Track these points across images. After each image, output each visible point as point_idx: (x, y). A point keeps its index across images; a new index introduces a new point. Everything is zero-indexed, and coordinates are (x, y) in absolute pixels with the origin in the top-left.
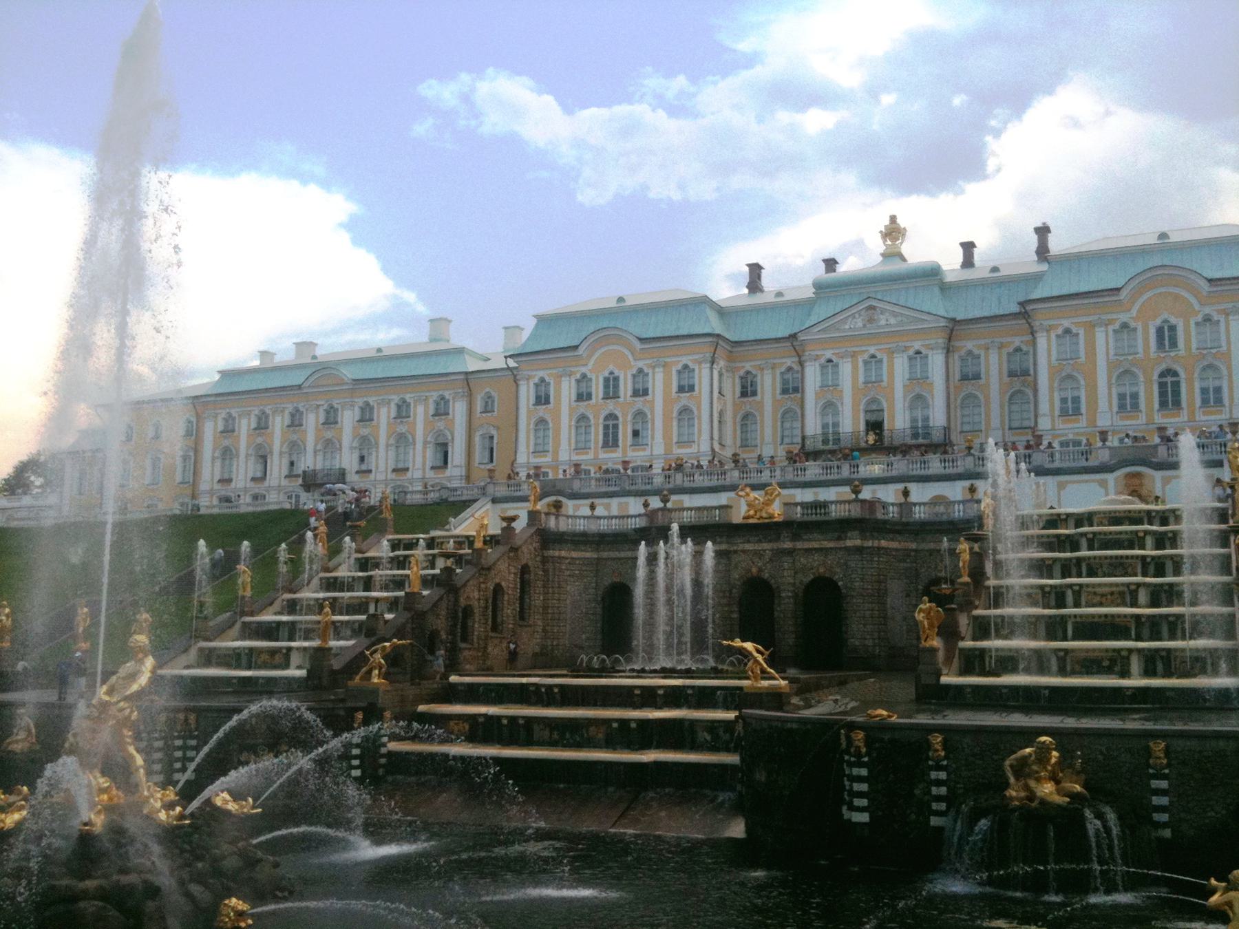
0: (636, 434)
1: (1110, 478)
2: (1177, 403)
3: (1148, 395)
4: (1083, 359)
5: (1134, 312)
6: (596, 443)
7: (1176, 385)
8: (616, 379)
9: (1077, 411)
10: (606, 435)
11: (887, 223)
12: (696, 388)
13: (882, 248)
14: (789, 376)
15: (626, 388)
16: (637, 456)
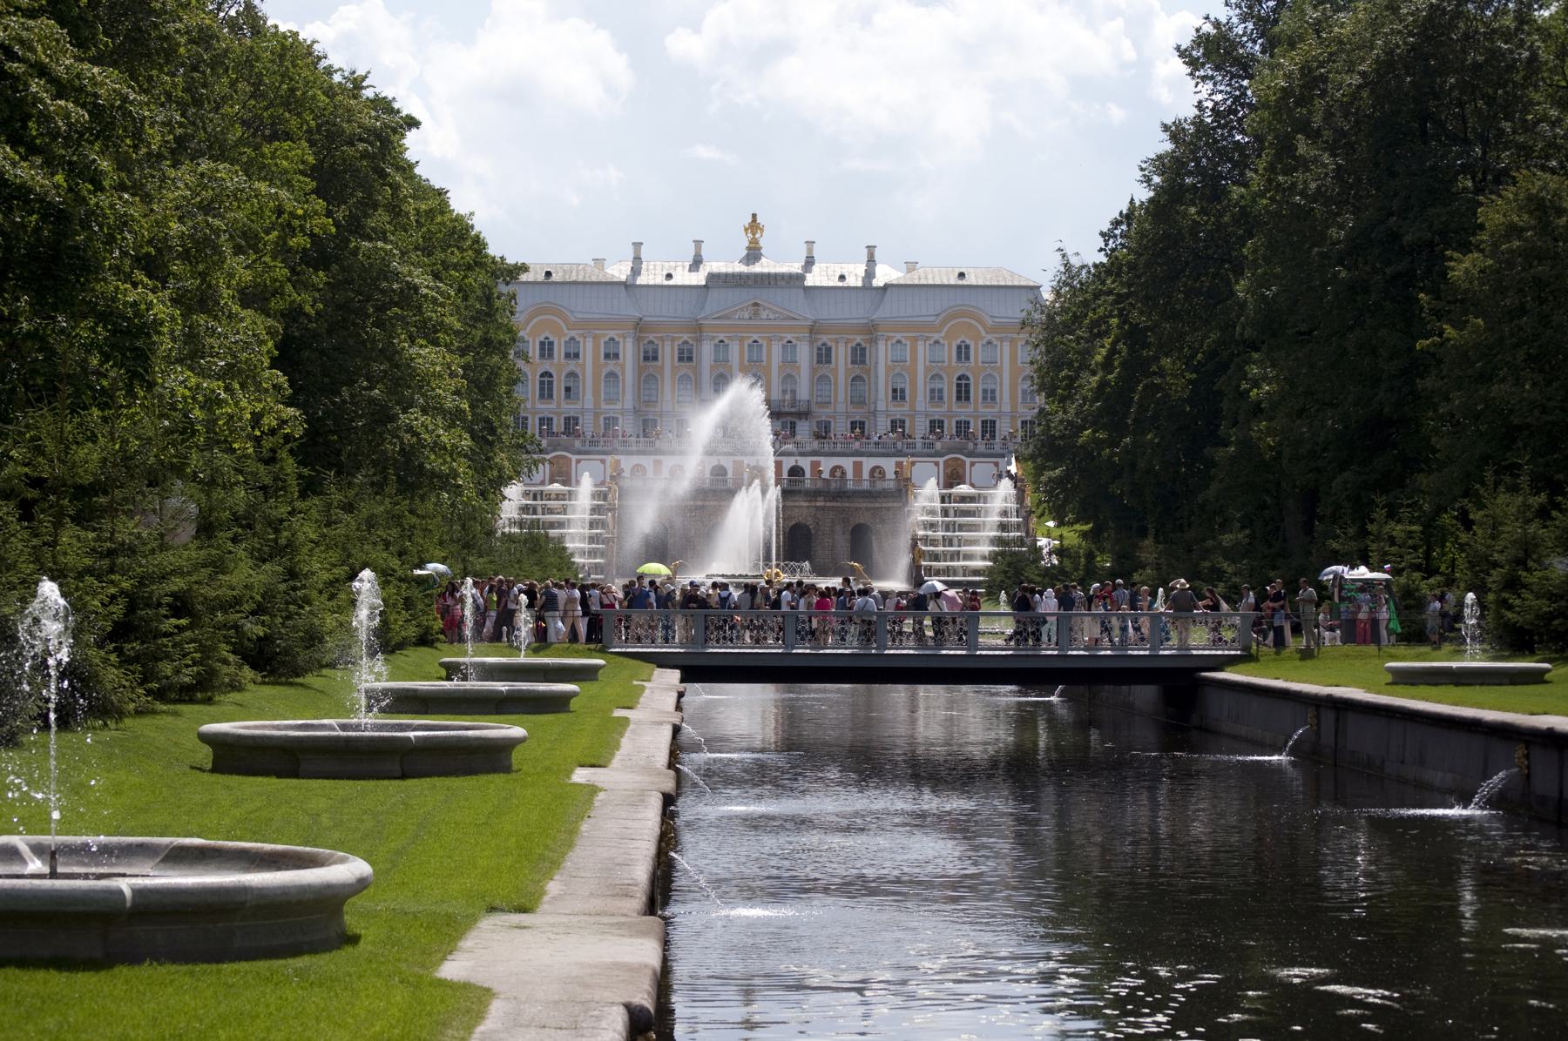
0: (568, 389)
1: (941, 460)
2: (967, 399)
3: (950, 391)
4: (908, 363)
5: (943, 334)
6: (533, 392)
7: (967, 386)
8: (551, 344)
9: (903, 398)
10: (542, 389)
11: (750, 220)
12: (621, 356)
13: (747, 244)
14: (685, 347)
15: (559, 351)
16: (570, 408)
